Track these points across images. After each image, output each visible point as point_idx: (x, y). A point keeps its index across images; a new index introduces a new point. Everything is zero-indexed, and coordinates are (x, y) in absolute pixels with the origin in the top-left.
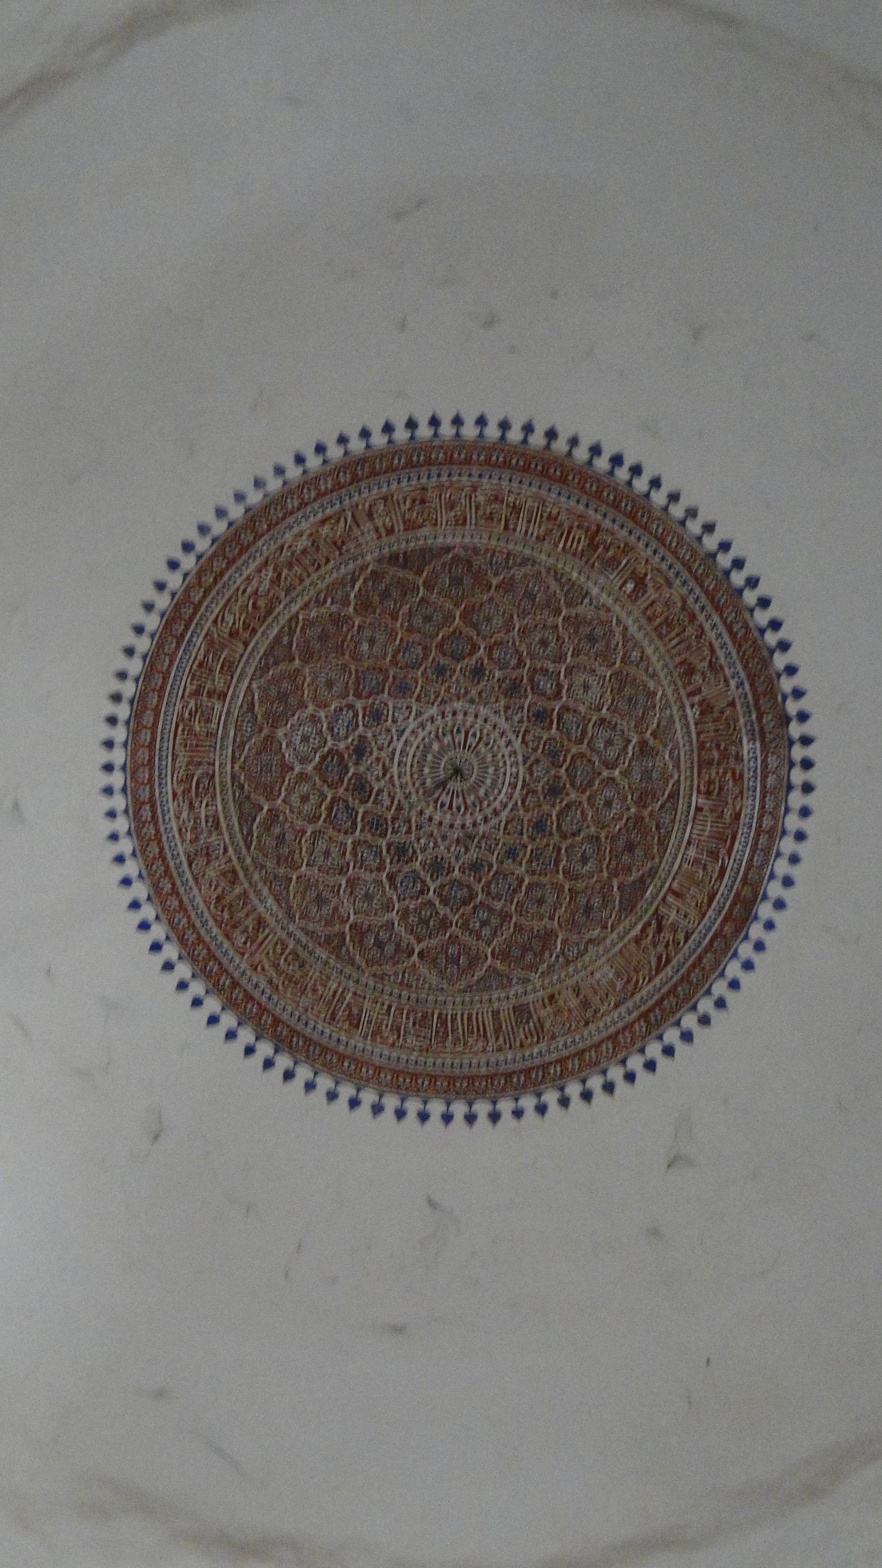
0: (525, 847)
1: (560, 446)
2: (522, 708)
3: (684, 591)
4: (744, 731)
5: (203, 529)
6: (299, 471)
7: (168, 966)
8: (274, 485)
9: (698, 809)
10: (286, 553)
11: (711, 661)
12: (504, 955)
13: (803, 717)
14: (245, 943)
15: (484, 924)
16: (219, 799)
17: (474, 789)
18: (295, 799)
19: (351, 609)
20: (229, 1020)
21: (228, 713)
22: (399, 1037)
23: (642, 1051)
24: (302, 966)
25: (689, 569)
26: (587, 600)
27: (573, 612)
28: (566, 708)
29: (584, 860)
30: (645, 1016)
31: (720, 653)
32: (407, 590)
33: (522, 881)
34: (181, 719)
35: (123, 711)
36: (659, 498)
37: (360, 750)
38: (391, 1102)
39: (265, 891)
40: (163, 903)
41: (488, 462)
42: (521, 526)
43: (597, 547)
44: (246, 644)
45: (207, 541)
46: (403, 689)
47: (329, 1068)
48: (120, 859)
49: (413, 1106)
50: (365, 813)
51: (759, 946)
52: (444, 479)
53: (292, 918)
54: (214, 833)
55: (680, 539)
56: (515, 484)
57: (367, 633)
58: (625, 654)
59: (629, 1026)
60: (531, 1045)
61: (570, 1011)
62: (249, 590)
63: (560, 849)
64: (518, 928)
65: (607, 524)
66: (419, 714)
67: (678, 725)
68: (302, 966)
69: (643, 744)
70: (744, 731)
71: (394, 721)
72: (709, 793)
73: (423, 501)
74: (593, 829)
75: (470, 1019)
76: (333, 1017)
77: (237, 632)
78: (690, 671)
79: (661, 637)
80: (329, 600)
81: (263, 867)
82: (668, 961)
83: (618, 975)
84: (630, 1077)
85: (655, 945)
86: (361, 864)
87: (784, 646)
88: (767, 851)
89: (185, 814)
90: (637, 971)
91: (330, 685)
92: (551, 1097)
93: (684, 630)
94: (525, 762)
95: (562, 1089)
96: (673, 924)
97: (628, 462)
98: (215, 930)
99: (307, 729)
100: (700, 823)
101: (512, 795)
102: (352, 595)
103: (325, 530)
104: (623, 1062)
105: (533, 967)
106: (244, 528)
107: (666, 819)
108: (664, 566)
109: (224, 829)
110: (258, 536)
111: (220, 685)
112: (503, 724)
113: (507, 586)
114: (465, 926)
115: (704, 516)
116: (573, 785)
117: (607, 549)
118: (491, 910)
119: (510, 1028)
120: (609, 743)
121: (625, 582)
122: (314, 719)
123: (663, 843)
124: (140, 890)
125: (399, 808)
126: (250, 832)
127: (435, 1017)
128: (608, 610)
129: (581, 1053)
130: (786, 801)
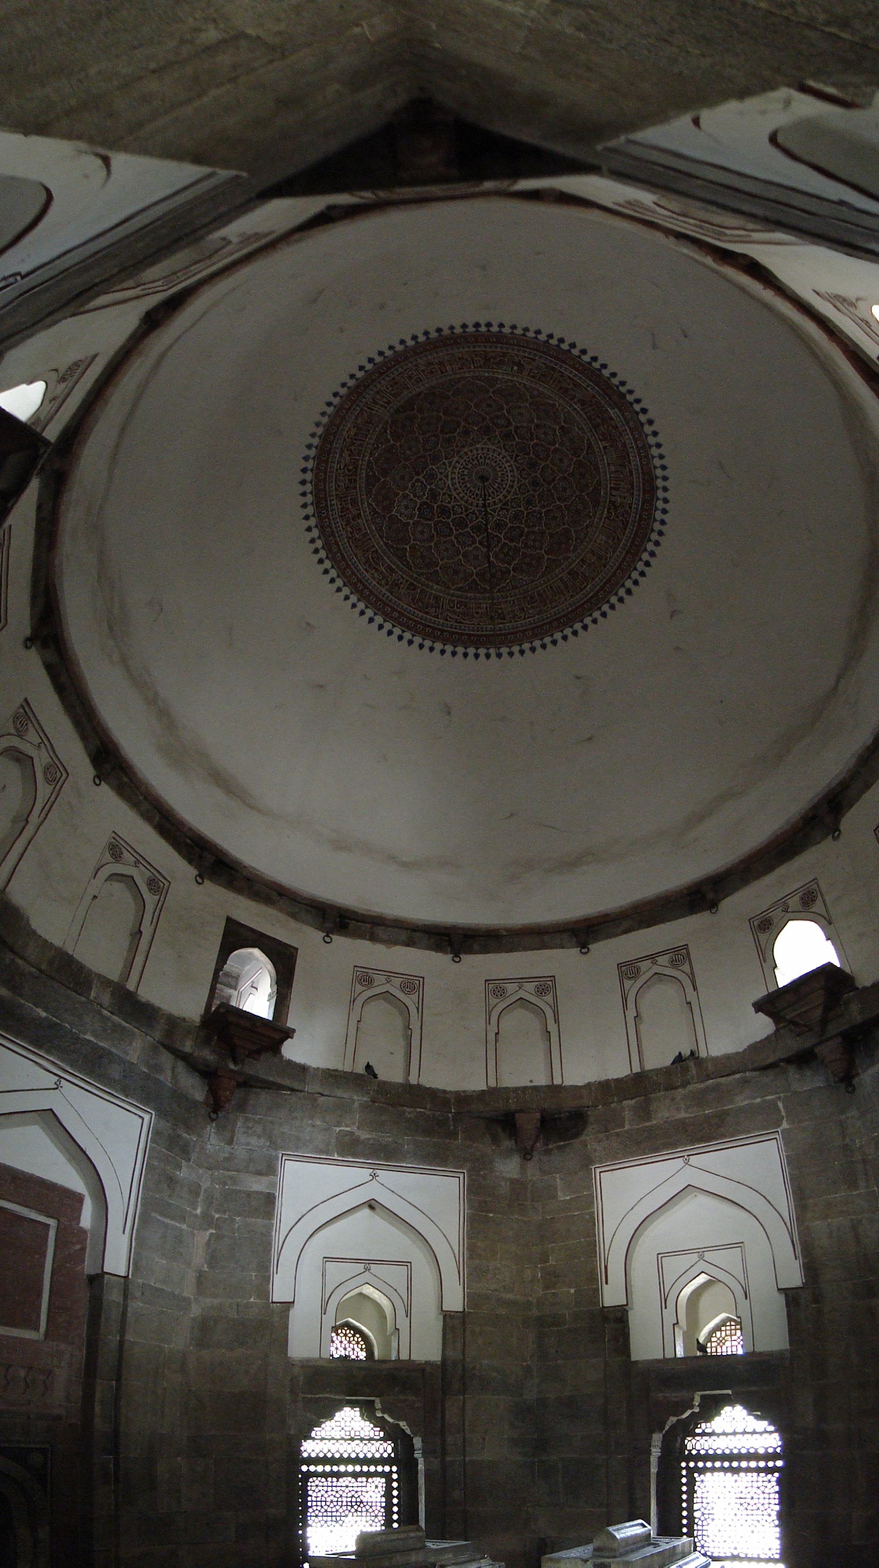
0: (534, 496)
2: (496, 436)
5: (306, 458)
7: (410, 642)
8: (325, 420)
9: (605, 448)
13: (631, 392)
14: (436, 611)
15: (534, 541)
16: (385, 558)
18: (418, 536)
19: (392, 442)
21: (366, 521)
23: (635, 569)
24: (466, 606)
26: (499, 382)
27: (495, 389)
28: (517, 427)
29: (564, 490)
34: (348, 538)
35: (323, 554)
37: (434, 495)
38: (537, 643)
39: (431, 584)
40: (391, 618)
42: (448, 368)
44: (355, 488)
45: (311, 461)
47: (502, 643)
48: (362, 613)
49: (548, 640)
51: (666, 501)
53: (448, 588)
56: (435, 355)
59: (624, 559)
60: (585, 587)
61: (594, 563)
62: (342, 467)
63: (550, 491)
65: (488, 349)
66: (450, 463)
68: (466, 606)
69: (562, 428)
71: (441, 473)
72: (605, 439)
73: (396, 383)
74: (561, 475)
75: (551, 587)
78: (566, 390)
79: (543, 382)
81: (422, 574)
82: (628, 522)
84: (636, 583)
85: (618, 517)
87: (604, 366)
88: (647, 456)
89: (376, 575)
91: (402, 478)
94: (512, 459)
95: (608, 602)
96: (621, 503)
98: (421, 614)
102: (389, 436)
103: (359, 421)
104: (630, 577)
108: (526, 354)
110: (332, 443)
111: (355, 512)
112: (494, 447)
114: (526, 546)
116: (541, 459)
117: (494, 358)
118: (534, 533)
122: (405, 497)
123: (597, 468)
124: (379, 619)
125: (467, 509)
126: (408, 562)
128: (512, 381)
129: (609, 581)
130: (644, 433)
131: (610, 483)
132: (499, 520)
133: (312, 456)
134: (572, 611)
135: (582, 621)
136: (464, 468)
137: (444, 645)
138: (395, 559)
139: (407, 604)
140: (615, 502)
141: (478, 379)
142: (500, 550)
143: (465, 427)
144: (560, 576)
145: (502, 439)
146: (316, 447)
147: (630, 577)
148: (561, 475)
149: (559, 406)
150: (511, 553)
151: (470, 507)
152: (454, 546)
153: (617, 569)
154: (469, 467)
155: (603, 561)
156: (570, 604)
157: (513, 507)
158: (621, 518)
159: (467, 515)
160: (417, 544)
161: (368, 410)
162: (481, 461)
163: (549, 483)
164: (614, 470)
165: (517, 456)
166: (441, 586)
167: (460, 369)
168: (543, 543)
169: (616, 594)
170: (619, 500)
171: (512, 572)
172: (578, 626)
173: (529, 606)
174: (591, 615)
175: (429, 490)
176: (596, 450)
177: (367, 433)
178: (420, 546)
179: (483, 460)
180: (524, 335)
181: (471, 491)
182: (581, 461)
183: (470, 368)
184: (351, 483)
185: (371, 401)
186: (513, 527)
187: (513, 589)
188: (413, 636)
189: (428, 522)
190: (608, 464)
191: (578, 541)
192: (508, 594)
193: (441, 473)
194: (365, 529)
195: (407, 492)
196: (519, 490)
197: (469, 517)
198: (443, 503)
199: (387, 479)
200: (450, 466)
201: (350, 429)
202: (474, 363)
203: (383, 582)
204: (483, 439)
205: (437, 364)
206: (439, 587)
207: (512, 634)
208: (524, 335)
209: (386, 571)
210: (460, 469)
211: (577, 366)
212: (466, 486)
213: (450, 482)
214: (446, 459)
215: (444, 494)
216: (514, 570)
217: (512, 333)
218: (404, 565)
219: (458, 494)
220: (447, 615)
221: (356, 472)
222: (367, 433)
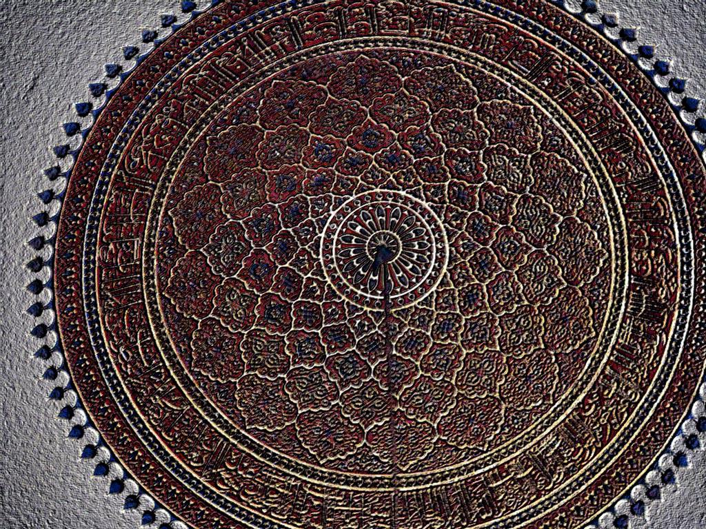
21: (150, 245)
28: (487, 188)
45: (104, 98)
63: (494, 320)
112: (426, 205)
131: (612, 354)
157: (412, 323)
213: (323, 235)
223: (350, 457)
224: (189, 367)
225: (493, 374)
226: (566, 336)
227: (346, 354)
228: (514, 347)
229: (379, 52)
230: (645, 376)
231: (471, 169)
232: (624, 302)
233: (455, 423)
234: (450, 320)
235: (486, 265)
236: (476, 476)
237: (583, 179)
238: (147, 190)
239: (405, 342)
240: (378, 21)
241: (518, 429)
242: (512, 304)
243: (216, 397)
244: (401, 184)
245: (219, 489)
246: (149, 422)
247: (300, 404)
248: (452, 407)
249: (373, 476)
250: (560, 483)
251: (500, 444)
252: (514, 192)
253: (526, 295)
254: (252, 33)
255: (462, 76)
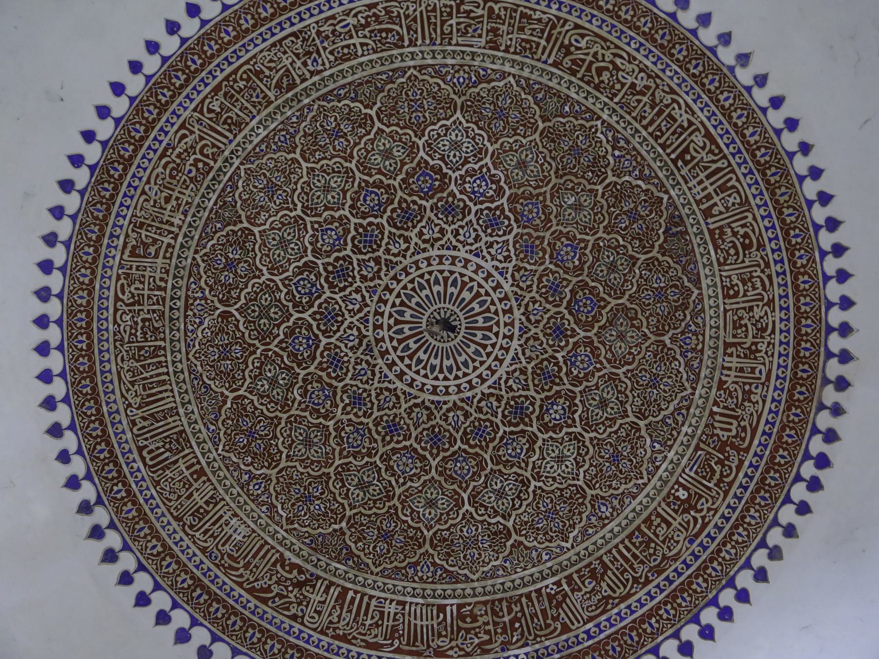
1: (830, 395)
3: (686, 556)
4: (537, 646)
6: (764, 102)
8: (745, 76)
9: (442, 609)
10: (668, 99)
11: (609, 597)
12: (240, 409)
14: (210, 111)
15: (273, 382)
17: (423, 345)
18: (383, 143)
19: (611, 178)
20: (120, 106)
21: (473, 54)
22: (127, 305)
23: (157, 587)
25: (712, 560)
26: (657, 446)
28: (533, 440)
29: (363, 486)
30: (198, 583)
31: (622, 606)
32: (644, 240)
33: (325, 417)
36: (787, 515)
37: (449, 210)
38: (54, 308)
41: (799, 315)
43: (722, 451)
44: (555, 64)
46: (527, 249)
47: (82, 230)
49: (53, 335)
50: (379, 226)
52: (775, 268)
53: (247, 159)
54: (332, 58)
55: (745, 545)
57: (587, 201)
58: (603, 498)
60: (143, 459)
63: (369, 455)
64: (274, 422)
65: (749, 458)
67: (534, 570)
70: (537, 646)
71: (491, 245)
72: (461, 617)
73: (745, 247)
74: (398, 491)
75: (163, 383)
76: (142, 225)
77: (568, 53)
79: (630, 537)
80: (617, 153)
81: (301, 118)
82: (264, 601)
83: (238, 546)
84: (126, 579)
85: (278, 583)
86: (321, 229)
89: (351, 20)
90: (246, 566)
91: (522, 165)
92: (88, 491)
93: (642, 562)
94: (462, 400)
95: (99, 501)
97: (823, 475)
98: (220, 76)
99: (467, 146)
100: (424, 611)
101: (422, 390)
102: (627, 178)
104: (141, 568)
105: (231, 446)
106: (690, 48)
107: (425, 572)
108: (710, 528)
109: (340, 68)
111: (504, 41)
112: (502, 372)
113: (662, 354)
114: (266, 359)
115: (772, 567)
117: (720, 462)
119: (160, 430)
120: (501, 494)
121: (686, 488)
125: (390, 265)
127: (158, 343)
128: (650, 473)
131: (356, 592)
132: (342, 322)
133: (680, 15)
134: (98, 410)
135: (72, 427)
136: (479, 294)
137: (132, 99)
138: (359, 74)
139: (254, 56)
140: (314, 587)
141: (678, 409)
142: (279, 301)
143: (572, 336)
144: (181, 411)
145: (513, 398)
146: (694, 32)
147: (141, 568)
148: (398, 491)
149: (562, 548)
150: (262, 321)
151: (392, 273)
152: (327, 208)
153: (164, 546)
154: (474, 305)
155: (188, 519)
156: (117, 412)
158: (276, 589)
159: (377, 260)
160: (369, 133)
161: (714, 166)
162: (479, 334)
163: (386, 458)
164: (386, 610)
165: (467, 415)
166: (257, 145)
167: (721, 383)
168: (262, 397)
169: (112, 526)
170: (316, 598)
171: (222, 308)
172: (63, 415)
173: (139, 320)
174: (79, 452)
175: (466, 206)
176: (439, 587)
177: (661, 141)
178: (361, 138)
179: (477, 339)
180: (763, 544)
181: (422, 288)
182: (420, 547)
183: (716, 403)
184: (574, 62)
185: (733, 182)
186: (317, 347)
187: (187, 296)
188: (184, 41)
189: (403, 176)
190: (399, 603)
191: (246, 477)
192: (183, 283)
193: (491, 245)
194: (457, 44)
195: (488, 160)
196: (387, 389)
197: (372, 264)
198: (423, 223)
199: (537, 136)
200: (497, 268)
201: (693, 113)
202: (721, 415)
203: (326, 28)
204: (530, 359)
205: (753, 343)
206: (256, 141)
207: (95, 260)
208: (763, 544)
209: (348, 46)
210: (480, 286)
211: (653, 620)
212: (437, 282)
213: (462, 254)
214: (517, 269)
215: (442, 231)
216: (226, 315)
217: (775, 523)
218: (343, 87)
219: (428, 259)
220: (192, 132)
221: (588, 83)
222: (661, 141)
223: (202, 290)
224: (318, 99)
225: (308, 458)
226: (365, 538)
227: (321, 285)
228: (342, 480)
229: (703, 310)
230: (338, 631)
231: (555, 419)
232: (421, 601)
233: (247, 416)
234: (365, 405)
235: (435, 443)
236: (189, 441)
237: (564, 544)
238: (543, 54)
239: (336, 354)
240: (744, 308)
241: (248, 490)
242: (393, 475)
243: (280, 131)
244: (526, 343)
245: (177, 132)
246: (261, 51)
247: (264, 231)
248: (265, 411)
249: (182, 319)
250: (194, 543)
251: (228, 470)
252: (532, 470)
253: (407, 490)
254: (733, 171)
255: (676, 402)
